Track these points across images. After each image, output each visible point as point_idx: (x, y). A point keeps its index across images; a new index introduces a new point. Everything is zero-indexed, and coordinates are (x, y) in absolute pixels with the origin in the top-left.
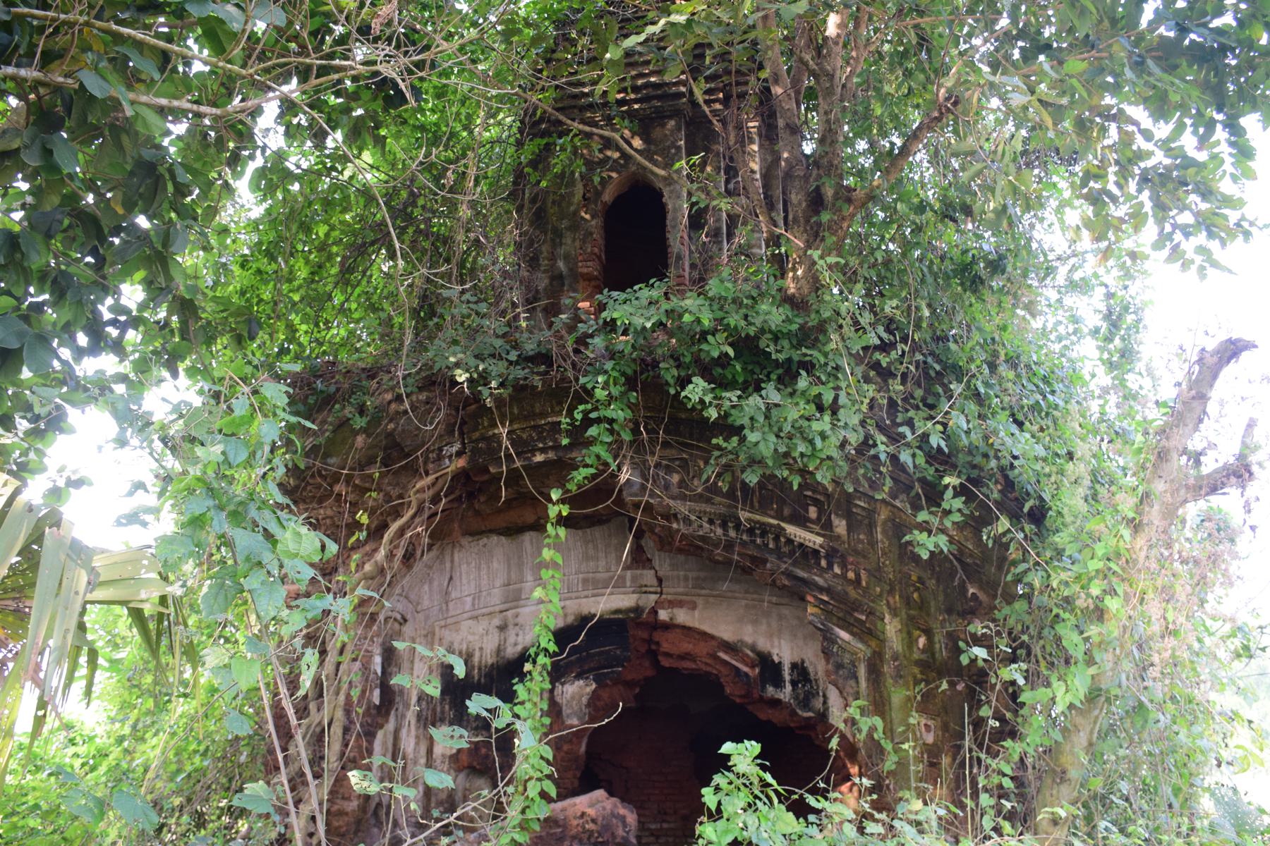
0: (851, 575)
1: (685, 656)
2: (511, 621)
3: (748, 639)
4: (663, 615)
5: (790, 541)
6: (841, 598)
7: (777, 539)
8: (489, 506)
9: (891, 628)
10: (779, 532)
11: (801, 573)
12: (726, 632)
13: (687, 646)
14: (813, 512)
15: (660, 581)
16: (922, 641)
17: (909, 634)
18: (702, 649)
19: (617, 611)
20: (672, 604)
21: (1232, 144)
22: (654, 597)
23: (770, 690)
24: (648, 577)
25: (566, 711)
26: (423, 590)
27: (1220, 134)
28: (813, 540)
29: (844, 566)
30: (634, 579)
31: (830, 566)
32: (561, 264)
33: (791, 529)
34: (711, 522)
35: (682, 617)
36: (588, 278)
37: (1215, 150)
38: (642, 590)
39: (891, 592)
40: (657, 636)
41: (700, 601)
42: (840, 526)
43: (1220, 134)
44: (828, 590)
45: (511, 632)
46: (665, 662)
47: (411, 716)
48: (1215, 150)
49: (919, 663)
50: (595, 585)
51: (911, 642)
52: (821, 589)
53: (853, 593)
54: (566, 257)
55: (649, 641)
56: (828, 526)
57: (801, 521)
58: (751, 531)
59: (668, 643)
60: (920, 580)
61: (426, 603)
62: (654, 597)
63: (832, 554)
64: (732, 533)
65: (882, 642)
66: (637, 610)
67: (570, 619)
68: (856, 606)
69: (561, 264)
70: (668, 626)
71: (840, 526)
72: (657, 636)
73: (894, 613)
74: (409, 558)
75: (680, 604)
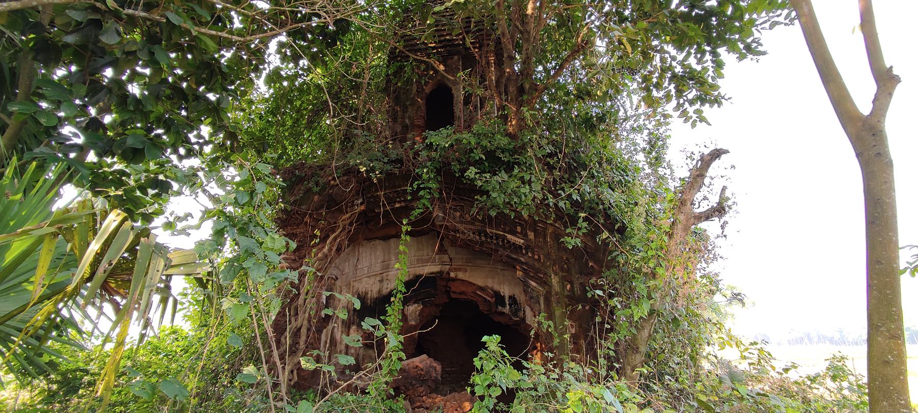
0: (536, 257)
1: (462, 293)
2: (385, 278)
3: (490, 285)
4: (452, 275)
5: (509, 242)
7: (503, 241)
8: (375, 228)
9: (555, 281)
10: (504, 238)
11: (514, 256)
12: (480, 282)
13: (463, 289)
14: (519, 229)
15: (451, 259)
16: (568, 286)
17: (563, 283)
18: (469, 290)
19: (432, 273)
20: (456, 270)
21: (713, 62)
22: (448, 267)
23: (500, 308)
24: (446, 258)
25: (409, 318)
26: (346, 266)
27: (708, 57)
29: (533, 253)
30: (439, 258)
31: (527, 253)
32: (407, 121)
33: (509, 236)
34: (474, 233)
35: (461, 275)
36: (419, 127)
37: (705, 65)
38: (442, 263)
39: (554, 264)
40: (450, 284)
41: (468, 268)
42: (531, 235)
43: (708, 57)
45: (385, 283)
46: (453, 296)
48: (705, 65)
49: (567, 297)
50: (423, 262)
51: (564, 287)
52: (523, 263)
53: (537, 265)
54: (409, 118)
55: (447, 286)
56: (526, 235)
57: (514, 233)
58: (491, 237)
59: (454, 287)
61: (347, 270)
62: (448, 267)
63: (528, 248)
64: (483, 238)
65: (551, 287)
66: (441, 272)
67: (411, 277)
68: (537, 271)
69: (407, 121)
70: (455, 280)
71: (531, 235)
72: (450, 284)
73: (556, 274)
74: (339, 250)
75: (460, 270)
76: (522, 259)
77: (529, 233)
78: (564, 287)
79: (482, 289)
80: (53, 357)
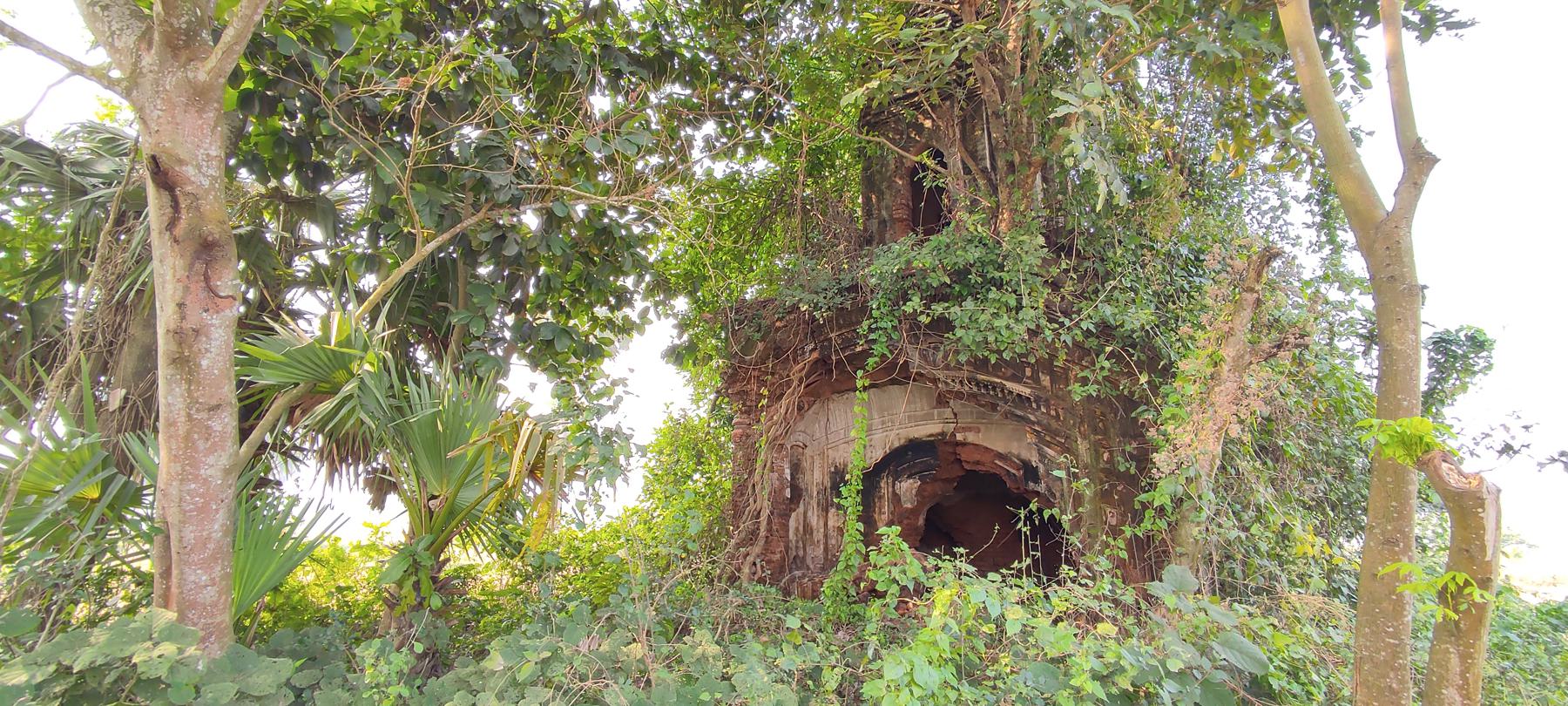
1: (978, 463)
3: (1015, 452)
4: (959, 437)
5: (1011, 393)
6: (1047, 429)
8: (831, 377)
9: (1082, 446)
11: (1019, 413)
13: (977, 457)
14: (1028, 372)
16: (1106, 456)
18: (986, 458)
20: (964, 429)
21: (1349, 61)
23: (1031, 484)
24: (948, 412)
27: (1337, 53)
28: (1026, 391)
29: (1048, 407)
33: (1009, 385)
37: (1336, 68)
40: (959, 450)
41: (982, 428)
43: (1337, 53)
44: (1039, 423)
46: (967, 467)
47: (814, 503)
48: (1336, 68)
49: (1103, 470)
51: (1098, 456)
53: (1054, 424)
56: (1037, 380)
57: (1016, 379)
58: (986, 387)
60: (1103, 414)
66: (943, 434)
68: (1055, 433)
70: (964, 444)
71: (1045, 380)
72: (959, 450)
73: (1084, 437)
75: (970, 429)
76: (1032, 418)
77: (1042, 377)
78: (1098, 456)
79: (1001, 456)
80: (1128, 531)
